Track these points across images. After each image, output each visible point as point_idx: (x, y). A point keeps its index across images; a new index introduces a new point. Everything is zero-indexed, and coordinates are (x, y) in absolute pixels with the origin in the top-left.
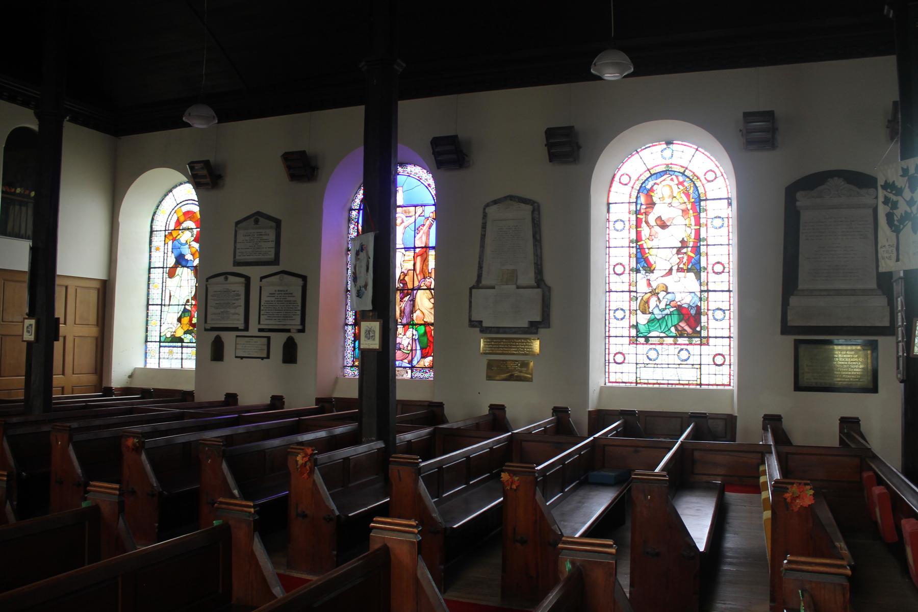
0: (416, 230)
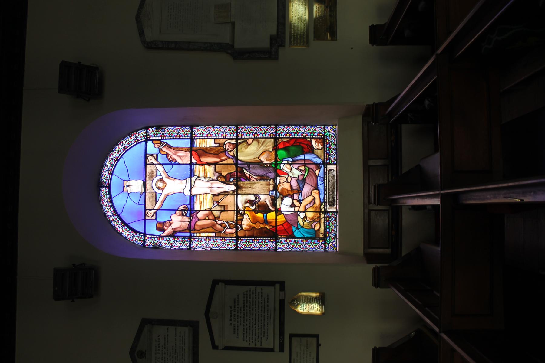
0: (173, 162)
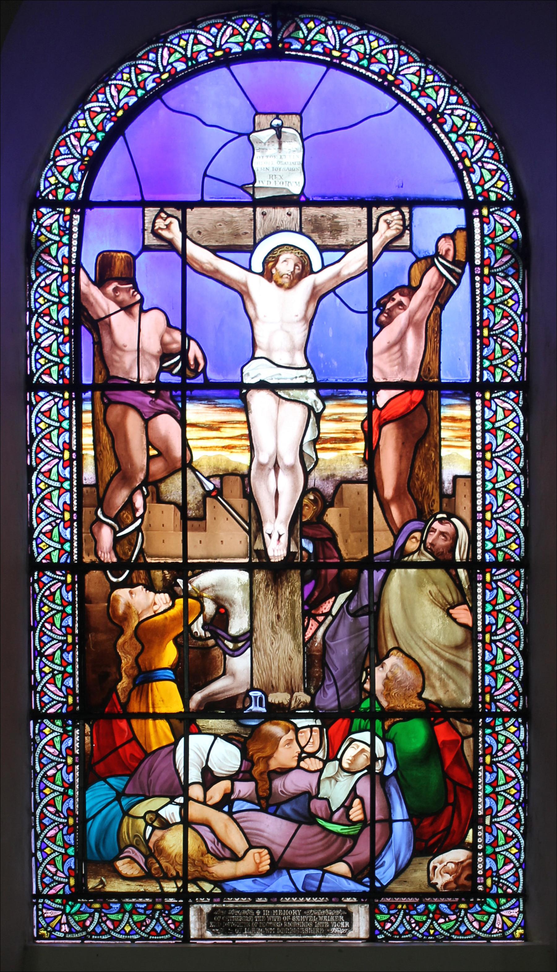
0: (378, 312)
